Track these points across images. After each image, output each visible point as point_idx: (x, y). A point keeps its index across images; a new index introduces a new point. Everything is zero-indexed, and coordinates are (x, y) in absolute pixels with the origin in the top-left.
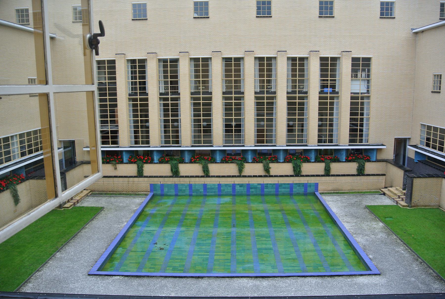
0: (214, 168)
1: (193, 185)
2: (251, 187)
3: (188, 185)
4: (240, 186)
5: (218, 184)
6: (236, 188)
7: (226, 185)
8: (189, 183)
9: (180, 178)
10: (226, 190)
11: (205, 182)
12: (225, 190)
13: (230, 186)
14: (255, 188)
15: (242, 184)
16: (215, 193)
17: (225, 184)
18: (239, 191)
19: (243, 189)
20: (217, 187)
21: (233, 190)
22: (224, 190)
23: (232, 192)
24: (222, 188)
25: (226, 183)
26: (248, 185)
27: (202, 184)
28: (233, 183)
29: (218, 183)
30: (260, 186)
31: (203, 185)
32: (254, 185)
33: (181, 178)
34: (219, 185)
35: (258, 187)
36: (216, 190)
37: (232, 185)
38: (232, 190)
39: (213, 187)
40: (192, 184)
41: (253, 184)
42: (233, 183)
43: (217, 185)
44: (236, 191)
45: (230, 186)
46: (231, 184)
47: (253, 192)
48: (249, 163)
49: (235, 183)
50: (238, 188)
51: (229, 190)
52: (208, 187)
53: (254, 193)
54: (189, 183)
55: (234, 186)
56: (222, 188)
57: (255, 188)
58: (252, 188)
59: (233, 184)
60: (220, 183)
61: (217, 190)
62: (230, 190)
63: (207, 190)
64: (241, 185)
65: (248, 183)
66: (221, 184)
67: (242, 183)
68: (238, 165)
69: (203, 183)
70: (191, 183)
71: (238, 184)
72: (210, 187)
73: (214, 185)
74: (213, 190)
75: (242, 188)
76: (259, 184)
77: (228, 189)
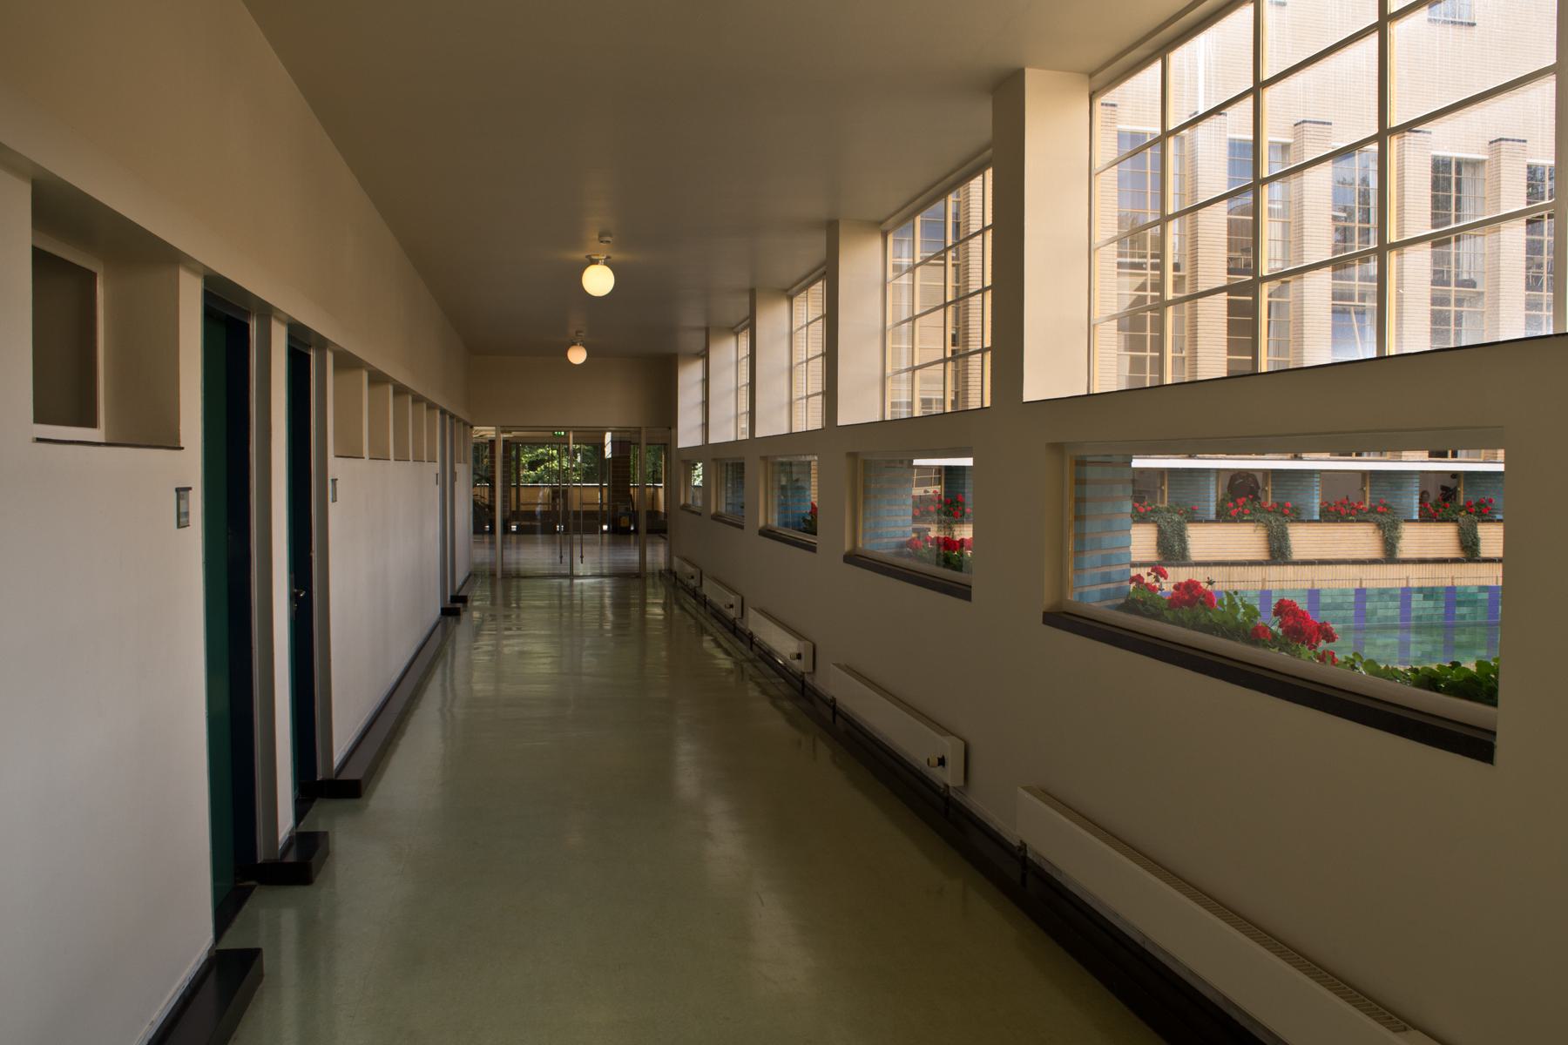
0: (1305, 539)
1: (1273, 595)
2: (1458, 599)
3: (1258, 593)
4: (1426, 598)
5: (1357, 590)
6: (1414, 605)
7: (1382, 593)
8: (1260, 588)
9: (1232, 568)
10: (1381, 613)
11: (1316, 582)
12: (1376, 612)
13: (1393, 597)
14: (1471, 601)
15: (1433, 588)
16: (1344, 621)
17: (1379, 589)
18: (1421, 613)
19: (1435, 608)
20: (1352, 599)
21: (1402, 613)
22: (1374, 612)
23: (1398, 619)
24: (1368, 605)
25: (1381, 586)
26: (1451, 590)
27: (1304, 589)
28: (1404, 584)
29: (1358, 586)
30: (1485, 596)
31: (1306, 593)
32: (1469, 591)
33: (1235, 568)
34: (1361, 593)
35: (1480, 597)
36: (1349, 612)
37: (1399, 592)
38: (1398, 610)
39: (1339, 600)
40: (1270, 589)
41: (1467, 587)
42: (1405, 586)
43: (1353, 593)
44: (1413, 614)
45: (1393, 597)
46: (1397, 589)
47: (1463, 617)
48: (1415, 521)
49: (1410, 585)
50: (1417, 602)
51: (1390, 613)
52: (1325, 600)
53: (1468, 620)
54: (1259, 586)
55: (1406, 593)
56: (1367, 604)
57: (1469, 601)
58: (1461, 604)
59: (1403, 589)
60: (1364, 586)
61: (1353, 612)
62: (1392, 610)
63: (1321, 612)
64: (1429, 593)
65: (1450, 585)
66: (1365, 589)
67: (1431, 585)
68: (1380, 529)
69: (1308, 585)
70: (1267, 588)
71: (1420, 590)
72: (1329, 600)
73: (1344, 593)
74: (1341, 613)
75: (1430, 604)
76: (1482, 589)
77: (1387, 608)
